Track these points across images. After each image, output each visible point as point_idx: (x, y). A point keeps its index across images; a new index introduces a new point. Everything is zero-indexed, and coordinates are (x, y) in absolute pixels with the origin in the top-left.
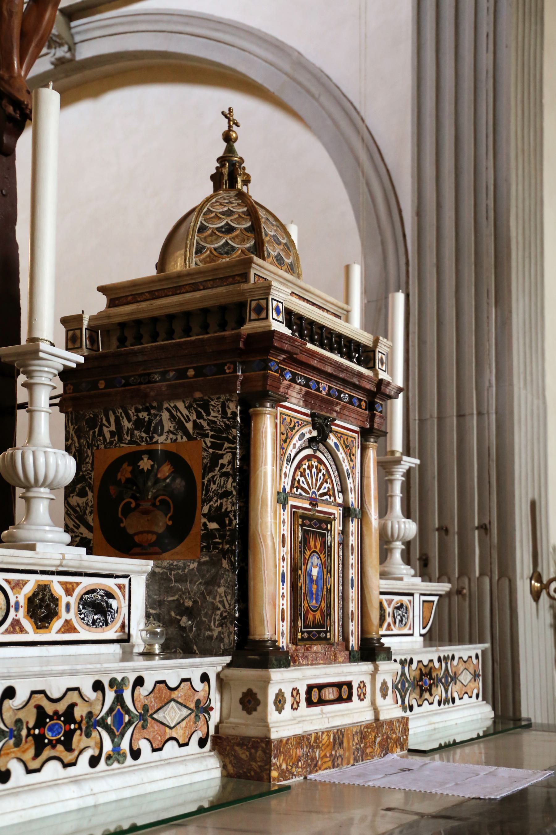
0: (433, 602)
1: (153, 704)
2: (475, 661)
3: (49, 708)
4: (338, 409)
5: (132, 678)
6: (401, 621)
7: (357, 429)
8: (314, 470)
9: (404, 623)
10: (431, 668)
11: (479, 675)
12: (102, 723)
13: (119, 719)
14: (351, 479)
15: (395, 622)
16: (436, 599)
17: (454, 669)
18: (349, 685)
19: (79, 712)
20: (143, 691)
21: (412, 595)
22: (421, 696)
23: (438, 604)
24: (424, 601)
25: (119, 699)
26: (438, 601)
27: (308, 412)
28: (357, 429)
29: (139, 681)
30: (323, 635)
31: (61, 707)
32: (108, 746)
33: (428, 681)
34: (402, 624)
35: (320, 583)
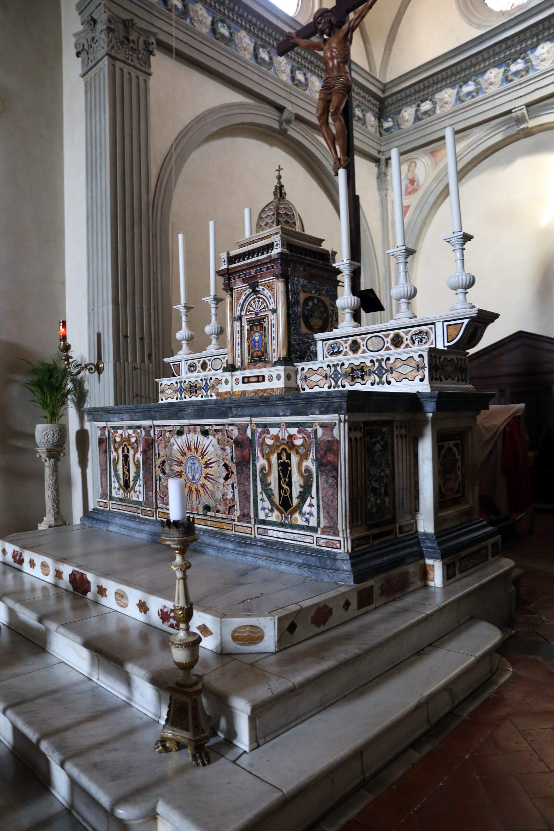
0: (463, 323)
1: (215, 384)
2: (417, 359)
3: (192, 385)
4: (259, 276)
5: (209, 378)
6: (421, 341)
7: (273, 278)
8: (260, 303)
9: (424, 341)
10: (363, 367)
11: (424, 367)
12: (203, 388)
13: (207, 387)
14: (272, 299)
15: (414, 343)
16: (466, 321)
17: (389, 366)
18: (263, 376)
19: (198, 386)
20: (212, 381)
21: (434, 324)
22: (353, 380)
23: (467, 325)
24: (447, 326)
25: (206, 383)
26: (469, 322)
27: (246, 284)
28: (273, 278)
29: (211, 379)
30: (263, 360)
31: (194, 384)
32: (205, 394)
33: (359, 373)
34: (421, 342)
35: (260, 342)
